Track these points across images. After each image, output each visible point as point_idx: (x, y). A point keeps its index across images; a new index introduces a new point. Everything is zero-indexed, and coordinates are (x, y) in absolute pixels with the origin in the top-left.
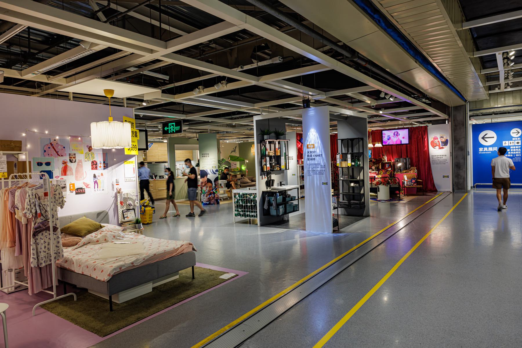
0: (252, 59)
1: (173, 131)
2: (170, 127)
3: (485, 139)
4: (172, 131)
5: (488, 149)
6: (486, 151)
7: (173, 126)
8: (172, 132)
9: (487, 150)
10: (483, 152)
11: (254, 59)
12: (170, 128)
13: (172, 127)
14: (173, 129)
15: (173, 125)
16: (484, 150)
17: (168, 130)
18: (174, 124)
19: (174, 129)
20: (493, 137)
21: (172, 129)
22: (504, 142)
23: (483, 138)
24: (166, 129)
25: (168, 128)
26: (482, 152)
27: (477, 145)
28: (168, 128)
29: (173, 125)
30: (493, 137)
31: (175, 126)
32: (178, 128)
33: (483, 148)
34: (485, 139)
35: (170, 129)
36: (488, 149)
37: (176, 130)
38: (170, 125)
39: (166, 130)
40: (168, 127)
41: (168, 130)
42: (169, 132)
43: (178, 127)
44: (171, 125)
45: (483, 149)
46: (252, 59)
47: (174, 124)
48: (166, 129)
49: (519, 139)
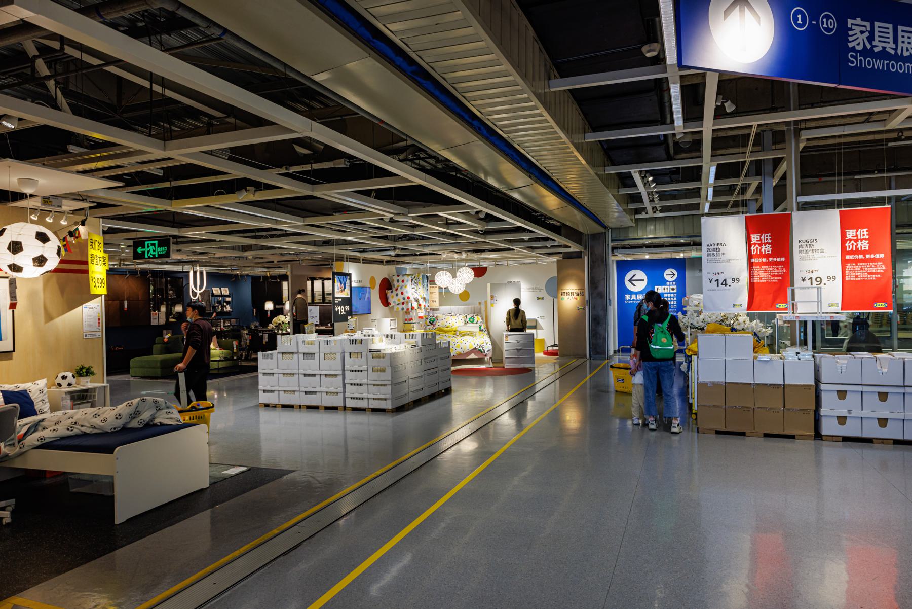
0: (294, 145)
1: (153, 255)
2: (148, 247)
3: (633, 282)
4: (151, 254)
5: (636, 297)
6: (634, 300)
7: (153, 247)
8: (151, 256)
9: (635, 298)
10: (631, 300)
11: (298, 145)
12: (148, 250)
13: (151, 248)
14: (154, 251)
15: (154, 245)
16: (632, 298)
17: (144, 252)
18: (156, 242)
19: (156, 251)
20: (643, 280)
21: (151, 251)
22: (656, 287)
23: (630, 281)
24: (140, 250)
25: (143, 250)
26: (629, 300)
27: (622, 290)
28: (143, 250)
29: (154, 245)
30: (643, 280)
31: (158, 247)
32: (163, 250)
33: (630, 295)
34: (633, 282)
35: (148, 252)
36: (636, 297)
37: (159, 253)
38: (148, 244)
39: (140, 252)
40: (144, 247)
41: (144, 252)
42: (146, 256)
43: (163, 248)
44: (150, 245)
45: (631, 297)
46: (294, 145)
47: (156, 242)
48: (140, 250)
49: (674, 283)
